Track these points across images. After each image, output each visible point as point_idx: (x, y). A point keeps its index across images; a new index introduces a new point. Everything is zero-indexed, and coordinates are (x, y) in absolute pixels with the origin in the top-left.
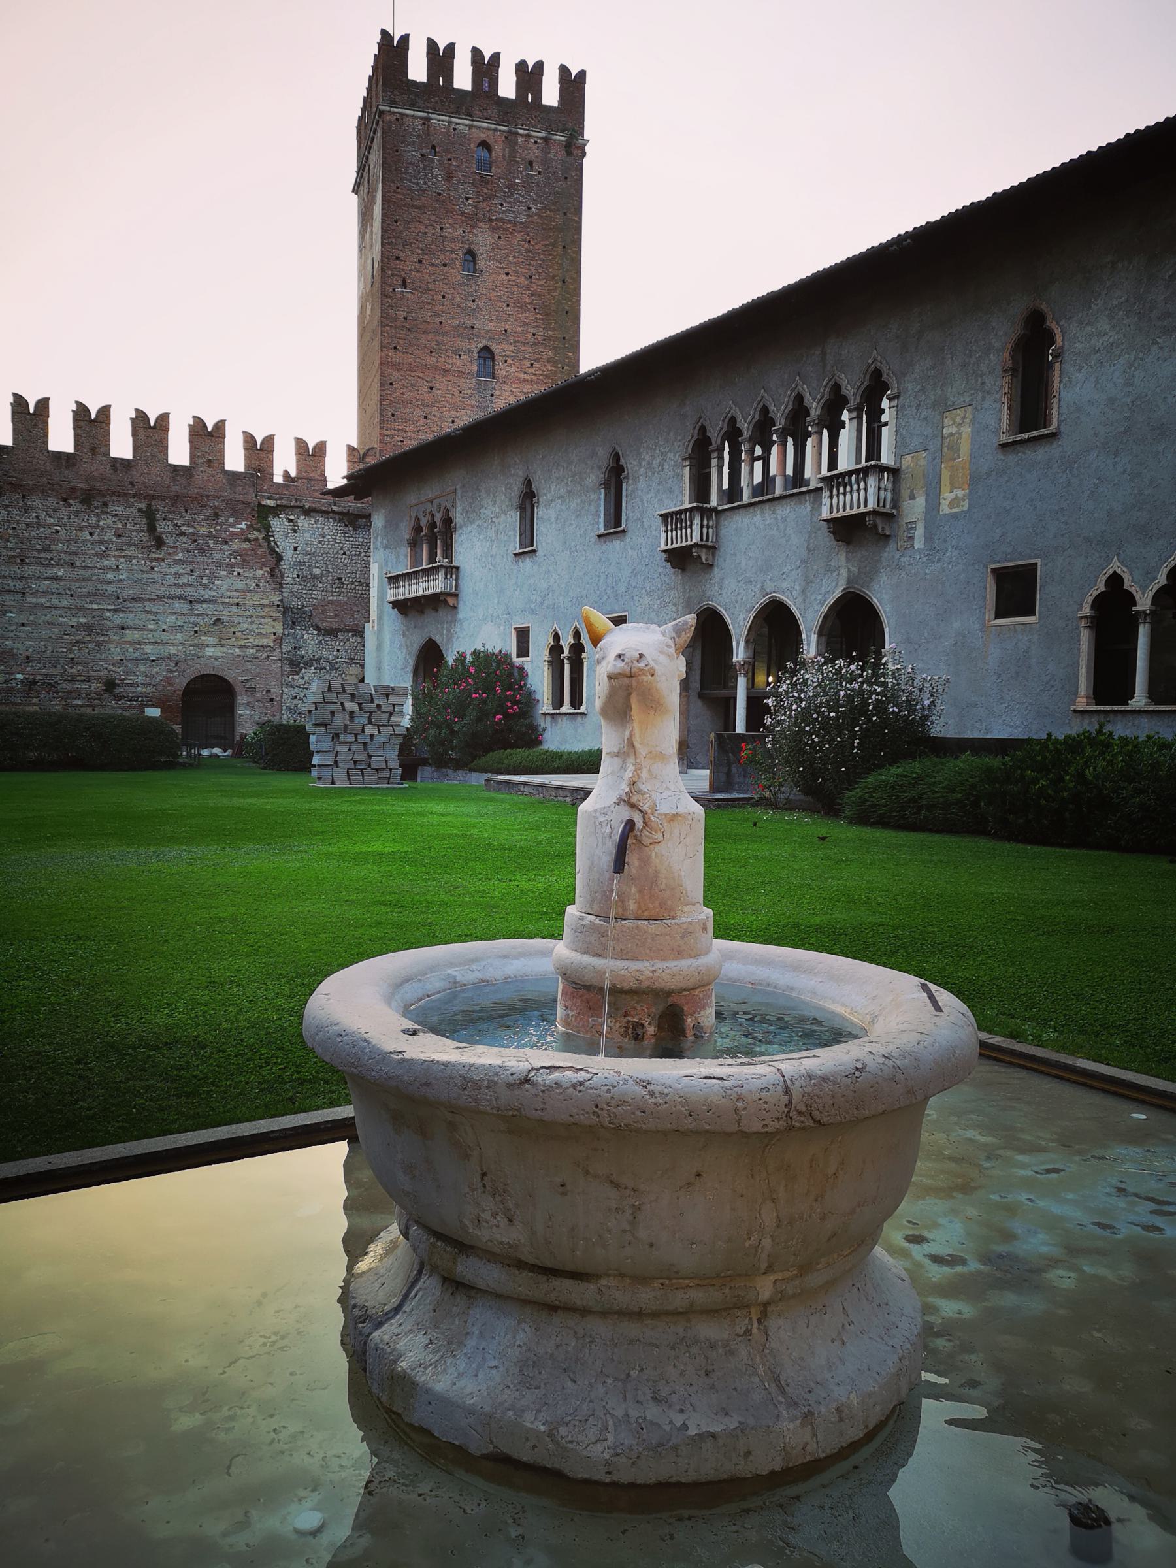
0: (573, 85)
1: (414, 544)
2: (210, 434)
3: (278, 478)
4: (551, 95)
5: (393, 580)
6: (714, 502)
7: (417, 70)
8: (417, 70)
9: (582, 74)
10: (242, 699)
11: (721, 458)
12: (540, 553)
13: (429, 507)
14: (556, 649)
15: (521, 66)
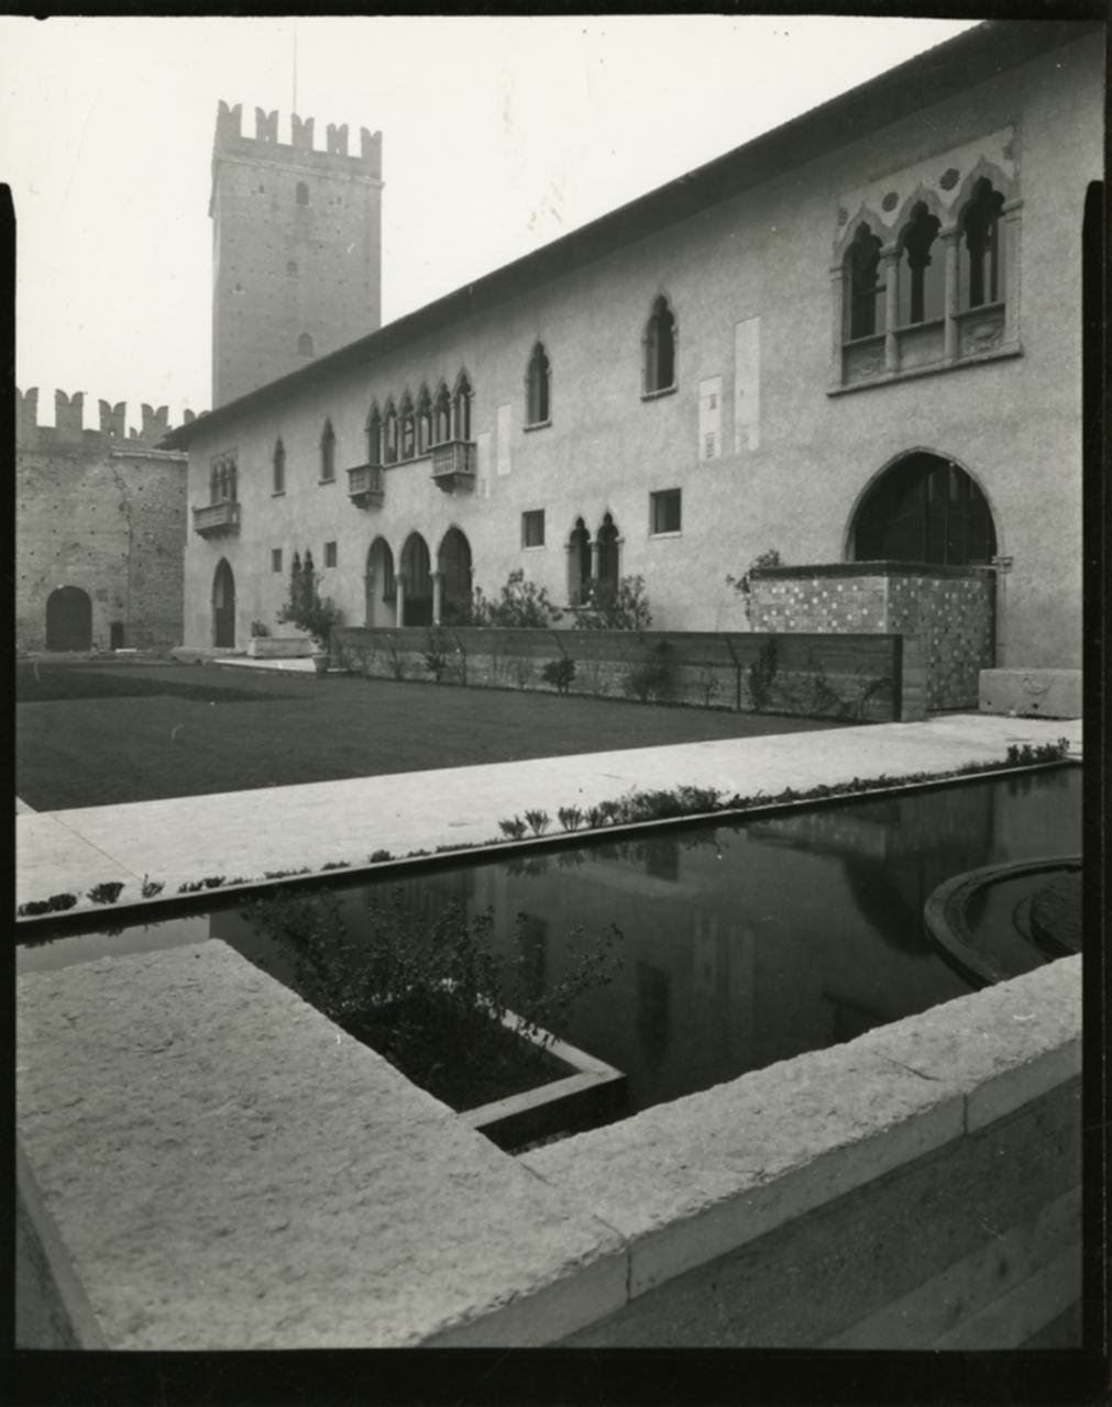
0: (372, 142)
1: (214, 486)
2: (72, 405)
3: (127, 434)
4: (354, 149)
5: (198, 513)
6: (382, 462)
7: (249, 129)
8: (249, 129)
9: (379, 134)
10: (98, 609)
11: (387, 432)
12: (287, 496)
13: (221, 459)
14: (296, 565)
15: (331, 129)
